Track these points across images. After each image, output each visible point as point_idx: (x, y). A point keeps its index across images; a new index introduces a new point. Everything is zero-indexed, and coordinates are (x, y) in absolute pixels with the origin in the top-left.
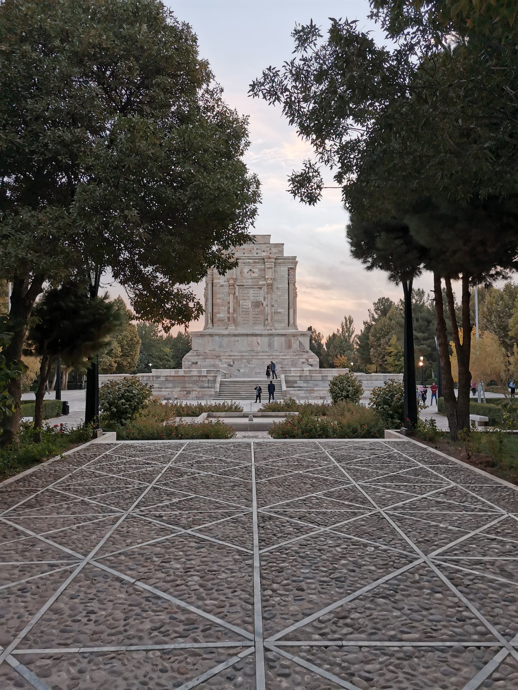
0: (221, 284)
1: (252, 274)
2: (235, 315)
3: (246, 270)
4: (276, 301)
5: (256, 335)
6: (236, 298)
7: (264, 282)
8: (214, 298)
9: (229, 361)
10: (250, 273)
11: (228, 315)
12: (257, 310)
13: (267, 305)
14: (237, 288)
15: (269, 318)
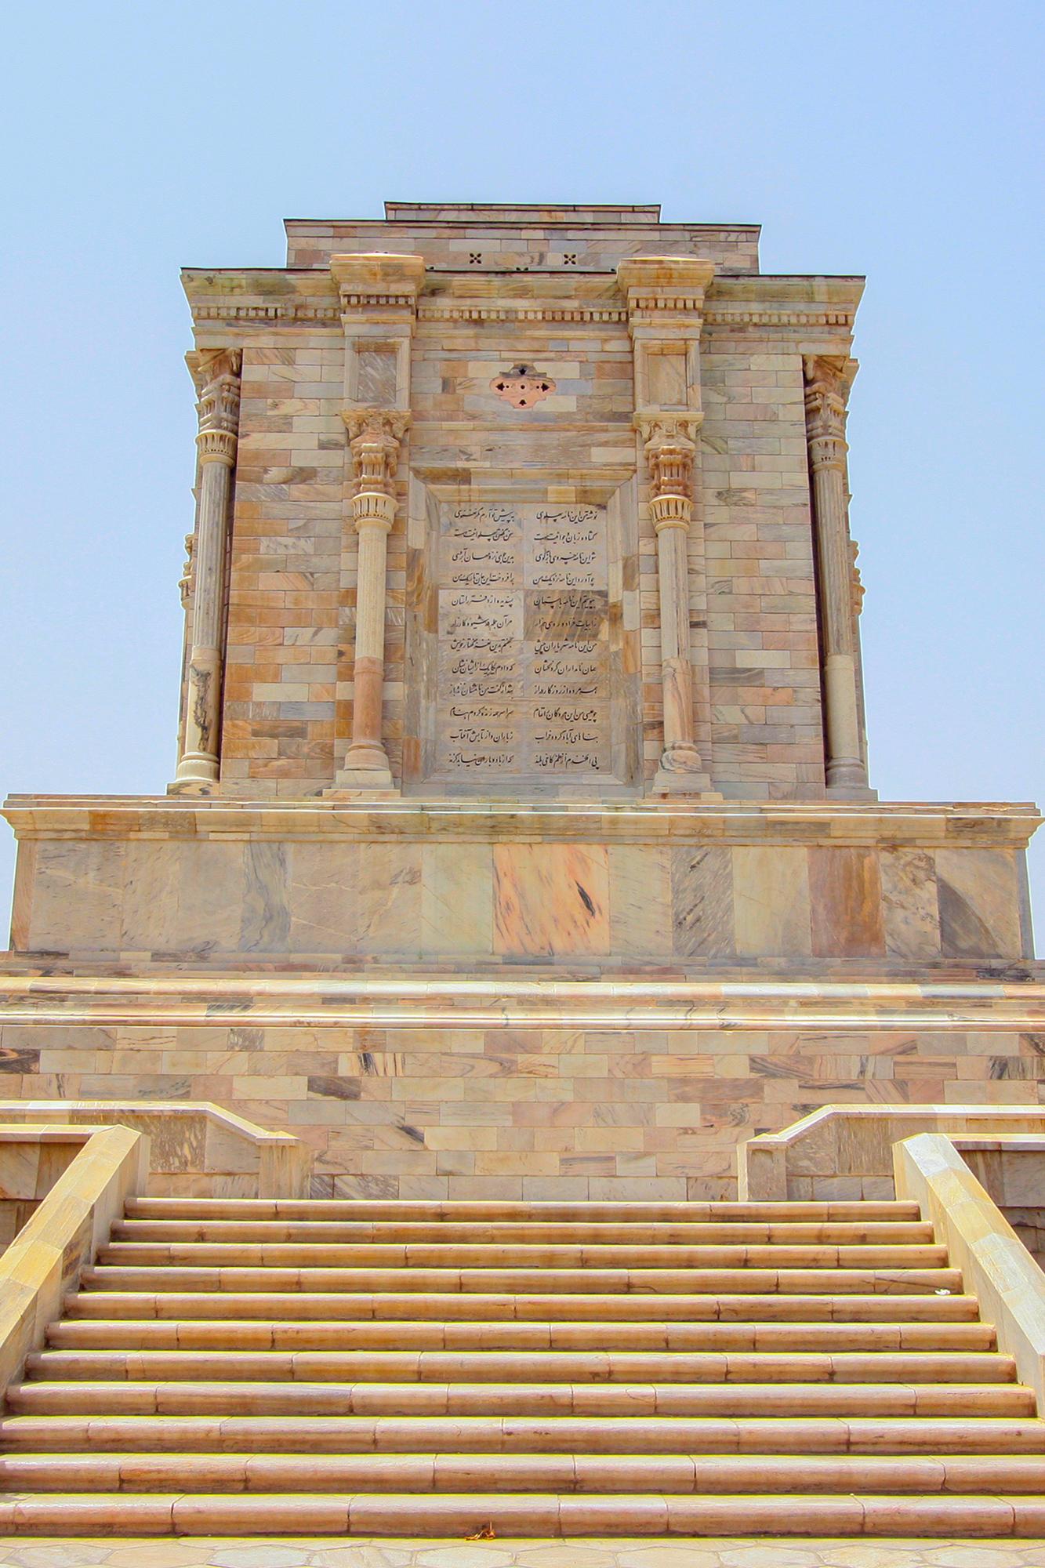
0: (298, 461)
1: (532, 394)
2: (397, 691)
3: (485, 370)
4: (725, 589)
5: (575, 832)
6: (406, 565)
7: (626, 454)
8: (241, 560)
9: (328, 1045)
10: (514, 387)
11: (343, 691)
12: (571, 657)
13: (653, 618)
14: (417, 491)
15: (672, 713)
